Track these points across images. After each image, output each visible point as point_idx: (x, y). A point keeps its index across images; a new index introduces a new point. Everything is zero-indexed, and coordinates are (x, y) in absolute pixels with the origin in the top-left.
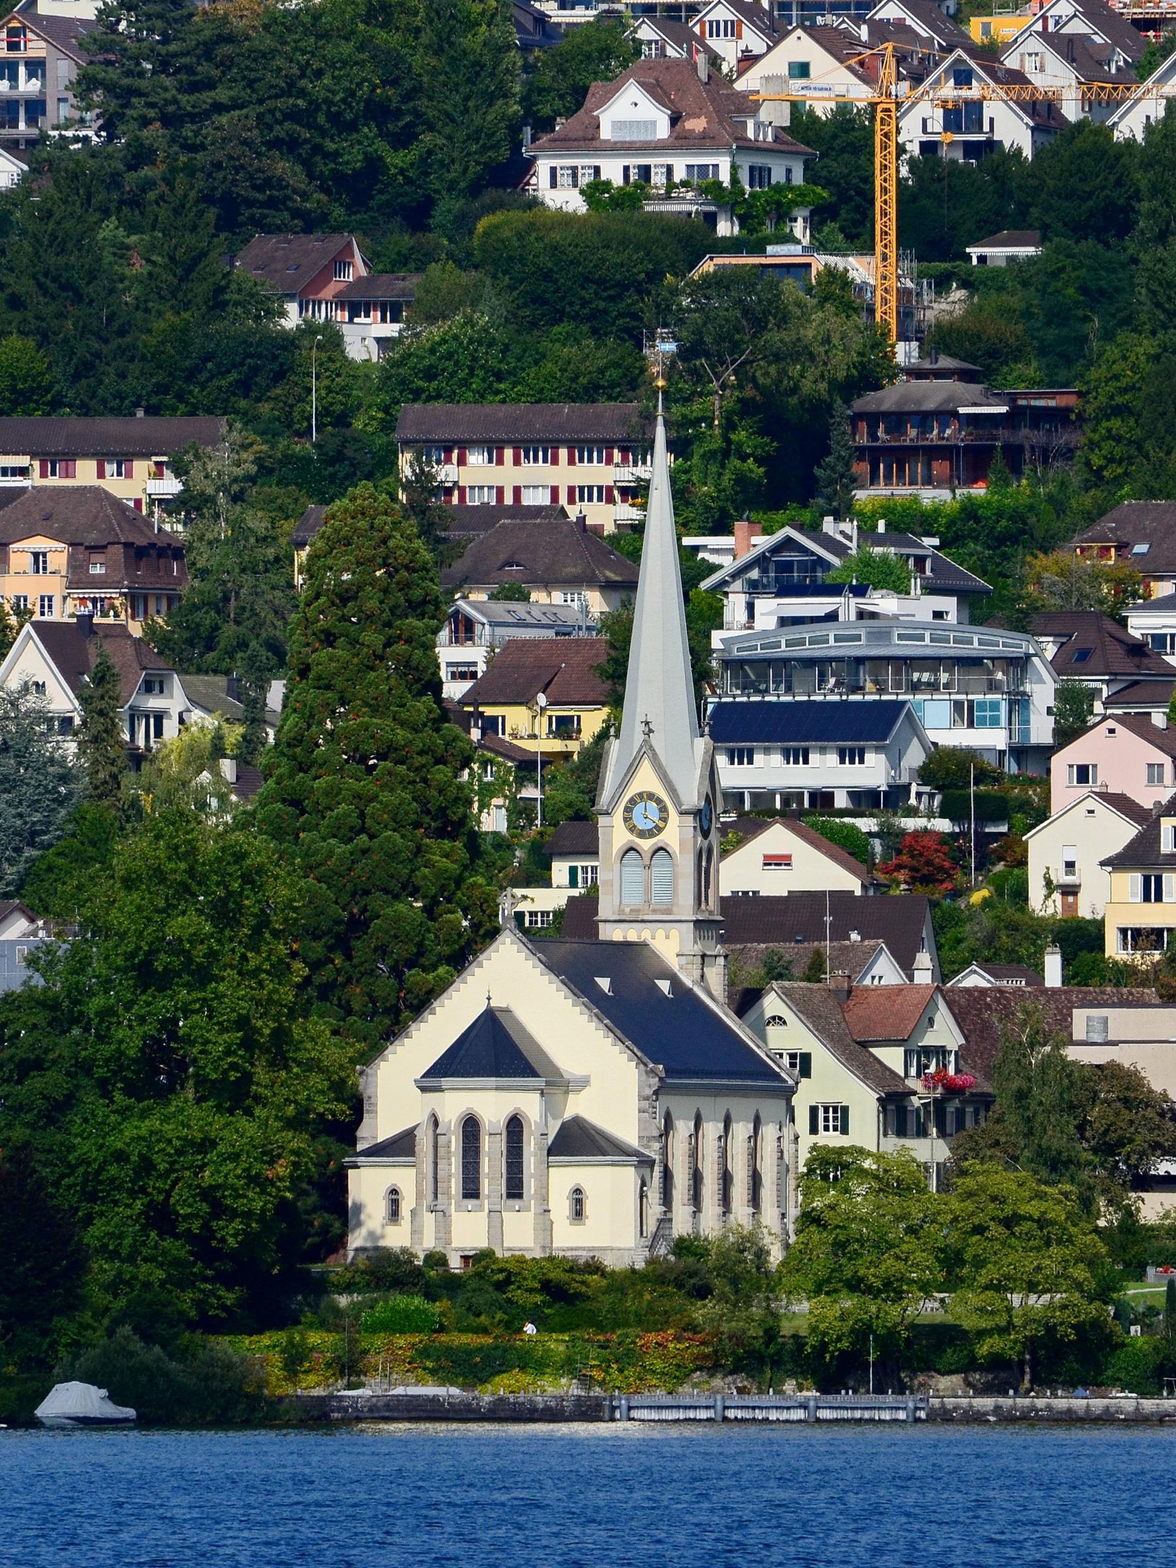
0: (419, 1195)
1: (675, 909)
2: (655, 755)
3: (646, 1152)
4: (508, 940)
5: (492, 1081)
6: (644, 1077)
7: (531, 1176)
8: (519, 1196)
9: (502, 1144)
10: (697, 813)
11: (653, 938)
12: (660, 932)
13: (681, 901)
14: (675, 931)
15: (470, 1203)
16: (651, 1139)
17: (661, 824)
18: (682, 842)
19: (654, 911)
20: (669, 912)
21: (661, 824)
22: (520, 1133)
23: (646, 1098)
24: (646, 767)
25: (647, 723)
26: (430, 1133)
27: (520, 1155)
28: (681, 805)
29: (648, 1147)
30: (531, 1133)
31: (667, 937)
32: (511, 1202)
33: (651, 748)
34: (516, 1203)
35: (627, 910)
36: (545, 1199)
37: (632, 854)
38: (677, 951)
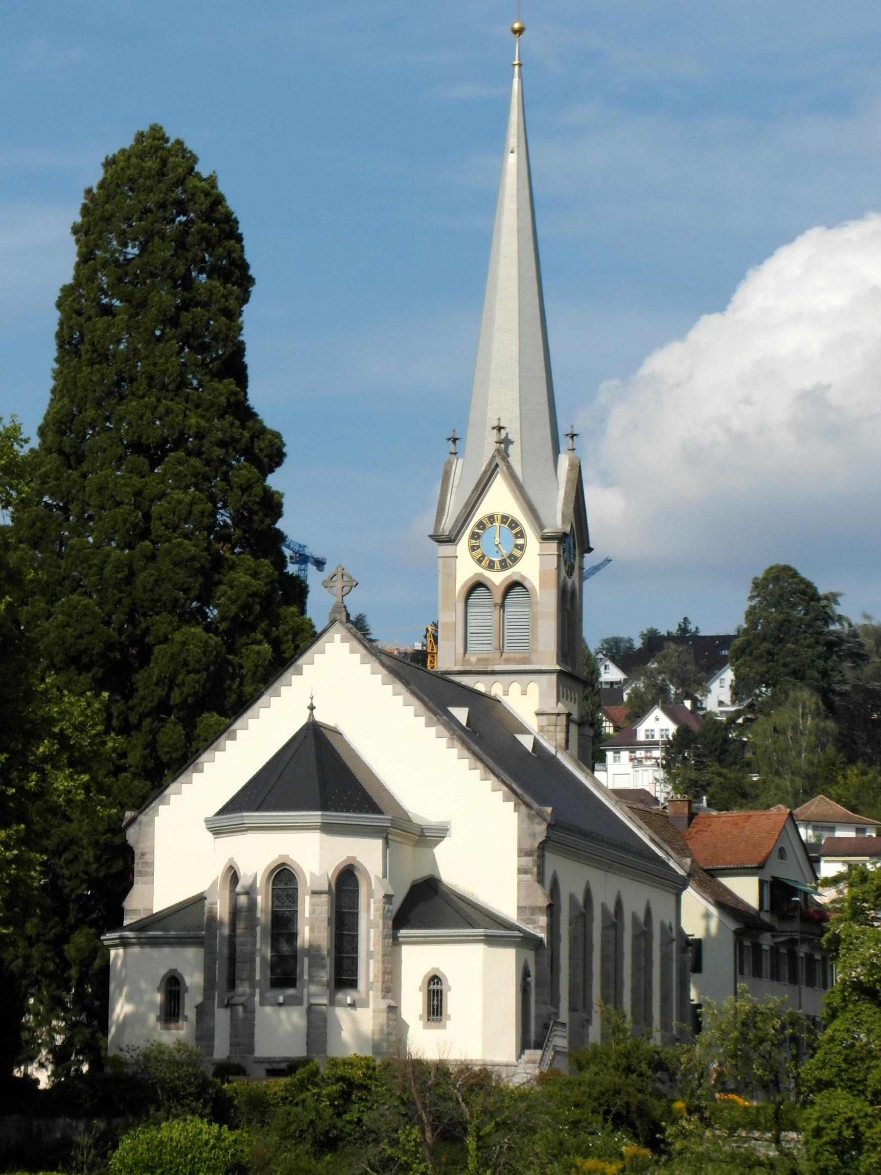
1: (534, 657)
2: (509, 467)
3: (529, 929)
4: (337, 637)
5: (315, 816)
6: (526, 824)
7: (370, 955)
8: (353, 984)
10: (561, 538)
11: (506, 693)
12: (515, 688)
16: (534, 910)
17: (517, 553)
18: (543, 574)
19: (508, 661)
20: (526, 661)
21: (517, 553)
22: (355, 893)
24: (499, 488)
25: (500, 429)
29: (534, 923)
30: (370, 895)
31: (524, 693)
35: (473, 659)
37: (480, 591)
38: (536, 707)
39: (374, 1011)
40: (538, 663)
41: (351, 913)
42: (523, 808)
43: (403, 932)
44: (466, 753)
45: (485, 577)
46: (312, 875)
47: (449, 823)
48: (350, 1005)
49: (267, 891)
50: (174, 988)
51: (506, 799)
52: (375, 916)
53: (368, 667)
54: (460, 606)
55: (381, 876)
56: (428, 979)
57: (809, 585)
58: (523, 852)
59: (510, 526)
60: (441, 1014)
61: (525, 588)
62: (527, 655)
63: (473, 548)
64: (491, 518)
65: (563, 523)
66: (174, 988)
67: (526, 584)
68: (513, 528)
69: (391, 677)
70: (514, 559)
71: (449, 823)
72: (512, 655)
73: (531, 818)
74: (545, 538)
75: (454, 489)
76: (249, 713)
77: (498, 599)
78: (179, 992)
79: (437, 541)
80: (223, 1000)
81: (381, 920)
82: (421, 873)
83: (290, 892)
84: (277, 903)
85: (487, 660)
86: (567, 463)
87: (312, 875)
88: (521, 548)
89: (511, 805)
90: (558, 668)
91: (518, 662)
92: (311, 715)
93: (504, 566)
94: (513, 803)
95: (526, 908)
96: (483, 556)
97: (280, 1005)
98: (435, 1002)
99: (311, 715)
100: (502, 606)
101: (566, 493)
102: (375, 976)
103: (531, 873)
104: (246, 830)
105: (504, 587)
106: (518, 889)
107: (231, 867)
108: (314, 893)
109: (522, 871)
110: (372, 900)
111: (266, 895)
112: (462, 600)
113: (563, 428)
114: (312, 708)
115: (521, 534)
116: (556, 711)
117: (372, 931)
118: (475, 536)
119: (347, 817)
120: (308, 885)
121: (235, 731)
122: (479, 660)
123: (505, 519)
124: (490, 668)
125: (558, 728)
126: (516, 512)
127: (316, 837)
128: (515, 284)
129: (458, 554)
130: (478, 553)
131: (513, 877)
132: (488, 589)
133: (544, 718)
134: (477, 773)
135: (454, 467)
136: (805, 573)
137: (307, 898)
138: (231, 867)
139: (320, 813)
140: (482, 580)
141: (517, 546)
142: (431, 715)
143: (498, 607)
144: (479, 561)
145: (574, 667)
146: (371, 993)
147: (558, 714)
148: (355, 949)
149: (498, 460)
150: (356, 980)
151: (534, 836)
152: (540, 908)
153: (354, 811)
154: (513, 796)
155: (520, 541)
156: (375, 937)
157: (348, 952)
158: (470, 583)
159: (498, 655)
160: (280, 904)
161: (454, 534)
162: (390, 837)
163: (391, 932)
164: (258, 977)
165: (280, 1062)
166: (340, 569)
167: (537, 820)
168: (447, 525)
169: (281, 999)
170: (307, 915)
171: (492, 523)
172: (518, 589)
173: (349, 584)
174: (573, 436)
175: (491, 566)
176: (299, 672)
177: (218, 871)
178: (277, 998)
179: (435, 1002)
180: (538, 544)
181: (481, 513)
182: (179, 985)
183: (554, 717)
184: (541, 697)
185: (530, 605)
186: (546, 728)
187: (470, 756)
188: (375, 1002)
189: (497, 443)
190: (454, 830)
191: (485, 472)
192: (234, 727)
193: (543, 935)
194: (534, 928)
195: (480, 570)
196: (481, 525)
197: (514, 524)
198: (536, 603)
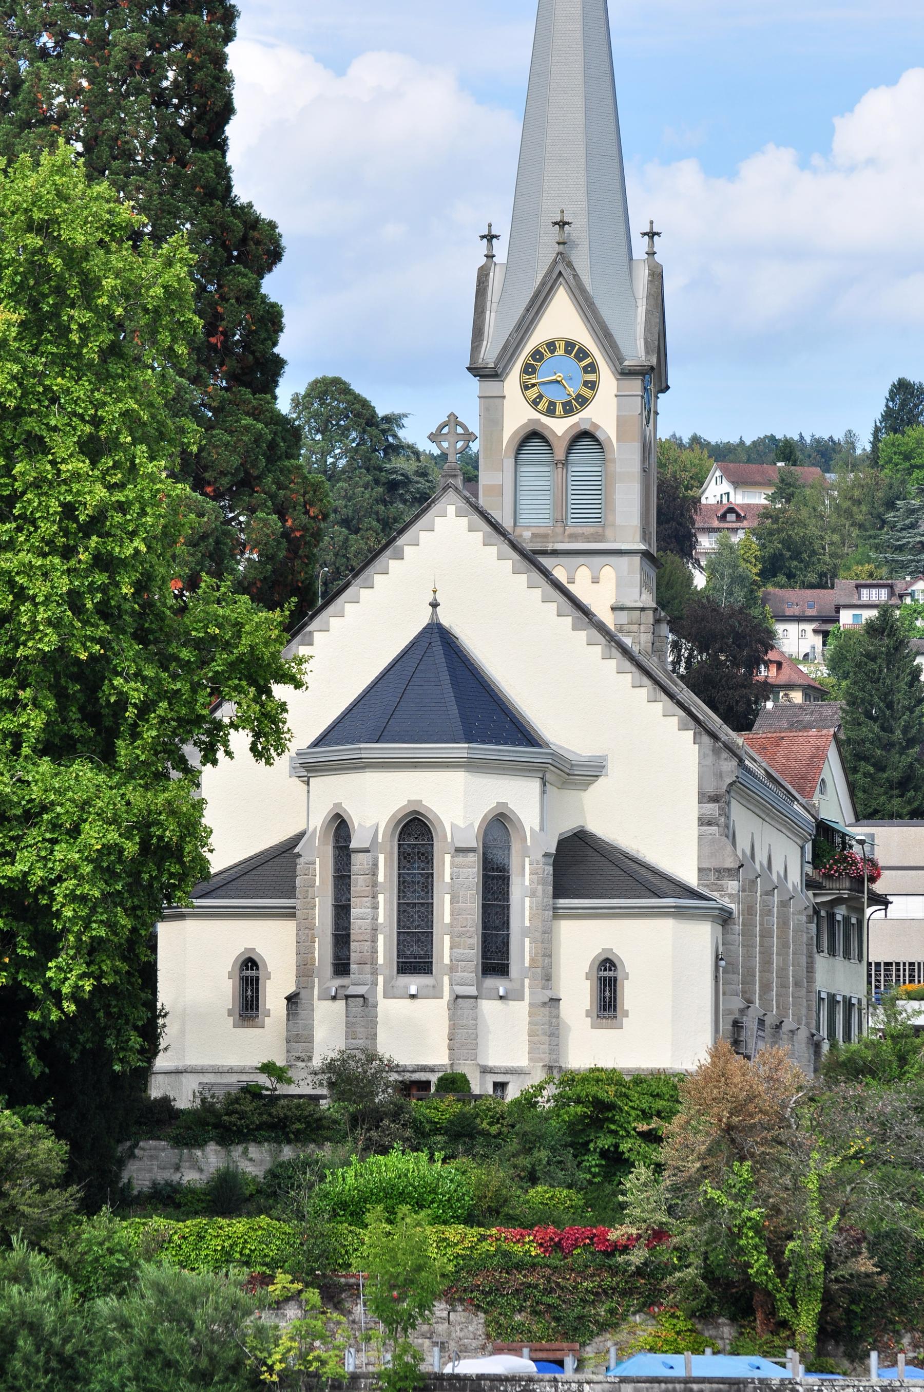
0: (304, 971)
1: (609, 533)
2: (576, 276)
4: (451, 509)
5: (460, 749)
6: (710, 760)
7: (525, 932)
9: (472, 869)
12: (583, 574)
13: (619, 520)
14: (608, 574)
15: (413, 983)
16: (722, 872)
17: (587, 392)
18: (621, 422)
19: (573, 537)
21: (587, 392)
23: (715, 799)
26: (329, 851)
27: (505, 894)
28: (621, 359)
29: (720, 889)
31: (595, 580)
32: (491, 982)
33: (570, 265)
34: (500, 985)
36: (547, 977)
37: (536, 445)
38: (612, 601)
39: (531, 1005)
40: (615, 541)
41: (500, 877)
42: (706, 739)
43: (562, 902)
44: (628, 665)
45: (543, 424)
46: (453, 825)
47: (604, 758)
48: (501, 998)
49: (392, 847)
50: (249, 973)
51: (683, 727)
52: (531, 881)
53: (494, 549)
54: (509, 463)
55: (537, 829)
56: (597, 963)
57: (365, 404)
58: (705, 797)
59: (576, 356)
60: (615, 1010)
61: (597, 440)
62: (600, 530)
63: (526, 387)
64: (551, 346)
65: (647, 353)
66: (249, 973)
67: (599, 434)
68: (580, 360)
69: (524, 564)
70: (583, 401)
71: (604, 758)
72: (579, 530)
73: (716, 752)
74: (625, 373)
75: (494, 305)
76: (331, 609)
77: (560, 454)
78: (257, 979)
79: (481, 376)
80: (329, 988)
81: (540, 887)
82: (568, 826)
83: (423, 850)
84: (404, 863)
85: (545, 536)
86: (647, 272)
87: (453, 825)
88: (592, 386)
89: (690, 734)
90: (643, 547)
91: (587, 539)
92: (434, 613)
93: (569, 410)
94: (692, 732)
95: (710, 870)
96: (540, 397)
97: (413, 997)
98: (607, 993)
99: (434, 613)
100: (565, 463)
101: (647, 312)
102: (532, 960)
103: (718, 825)
104: (364, 768)
105: (568, 437)
106: (699, 845)
107: (338, 816)
108: (459, 851)
109: (704, 822)
110: (527, 860)
111: (392, 853)
112: (513, 455)
113: (638, 225)
114: (434, 605)
115: (592, 368)
116: (640, 605)
117: (527, 900)
118: (529, 369)
119: (499, 750)
120: (449, 840)
121: (311, 633)
122: (534, 536)
123: (570, 345)
124: (550, 547)
125: (642, 628)
126: (585, 338)
127: (458, 778)
128: (579, 26)
129: (506, 393)
130: (533, 393)
131: (692, 830)
132: (547, 441)
133: (624, 614)
134: (643, 693)
135: (491, 274)
136: (359, 388)
137: (448, 858)
138: (338, 816)
139: (466, 745)
140: (539, 429)
141: (586, 384)
142: (580, 614)
143: (560, 466)
144: (535, 403)
145: (650, 545)
146: (527, 981)
147: (643, 609)
148: (506, 924)
149: (561, 267)
150: (508, 965)
151: (720, 776)
152: (729, 870)
153: (505, 743)
154: (692, 723)
155: (591, 377)
156: (531, 908)
157: (497, 928)
158: (522, 434)
159: (559, 530)
160: (408, 865)
161: (501, 365)
162: (548, 777)
163: (551, 901)
164: (381, 960)
165: (414, 1071)
166: (452, 418)
167: (725, 755)
168: (489, 354)
169: (413, 990)
170: (447, 879)
171: (552, 352)
172: (587, 442)
173: (467, 437)
174: (652, 235)
175: (550, 411)
176: (400, 556)
177: (318, 820)
178: (407, 988)
179: (607, 993)
180: (615, 382)
181: (537, 338)
182: (258, 969)
183: (637, 613)
184: (618, 585)
185: (604, 462)
186: (626, 627)
187: (634, 669)
188: (531, 994)
189: (559, 243)
190: (612, 767)
191: (543, 284)
192: (308, 629)
193: (732, 906)
194: (722, 896)
195: (537, 416)
196: (537, 355)
197: (582, 354)
198: (614, 461)
